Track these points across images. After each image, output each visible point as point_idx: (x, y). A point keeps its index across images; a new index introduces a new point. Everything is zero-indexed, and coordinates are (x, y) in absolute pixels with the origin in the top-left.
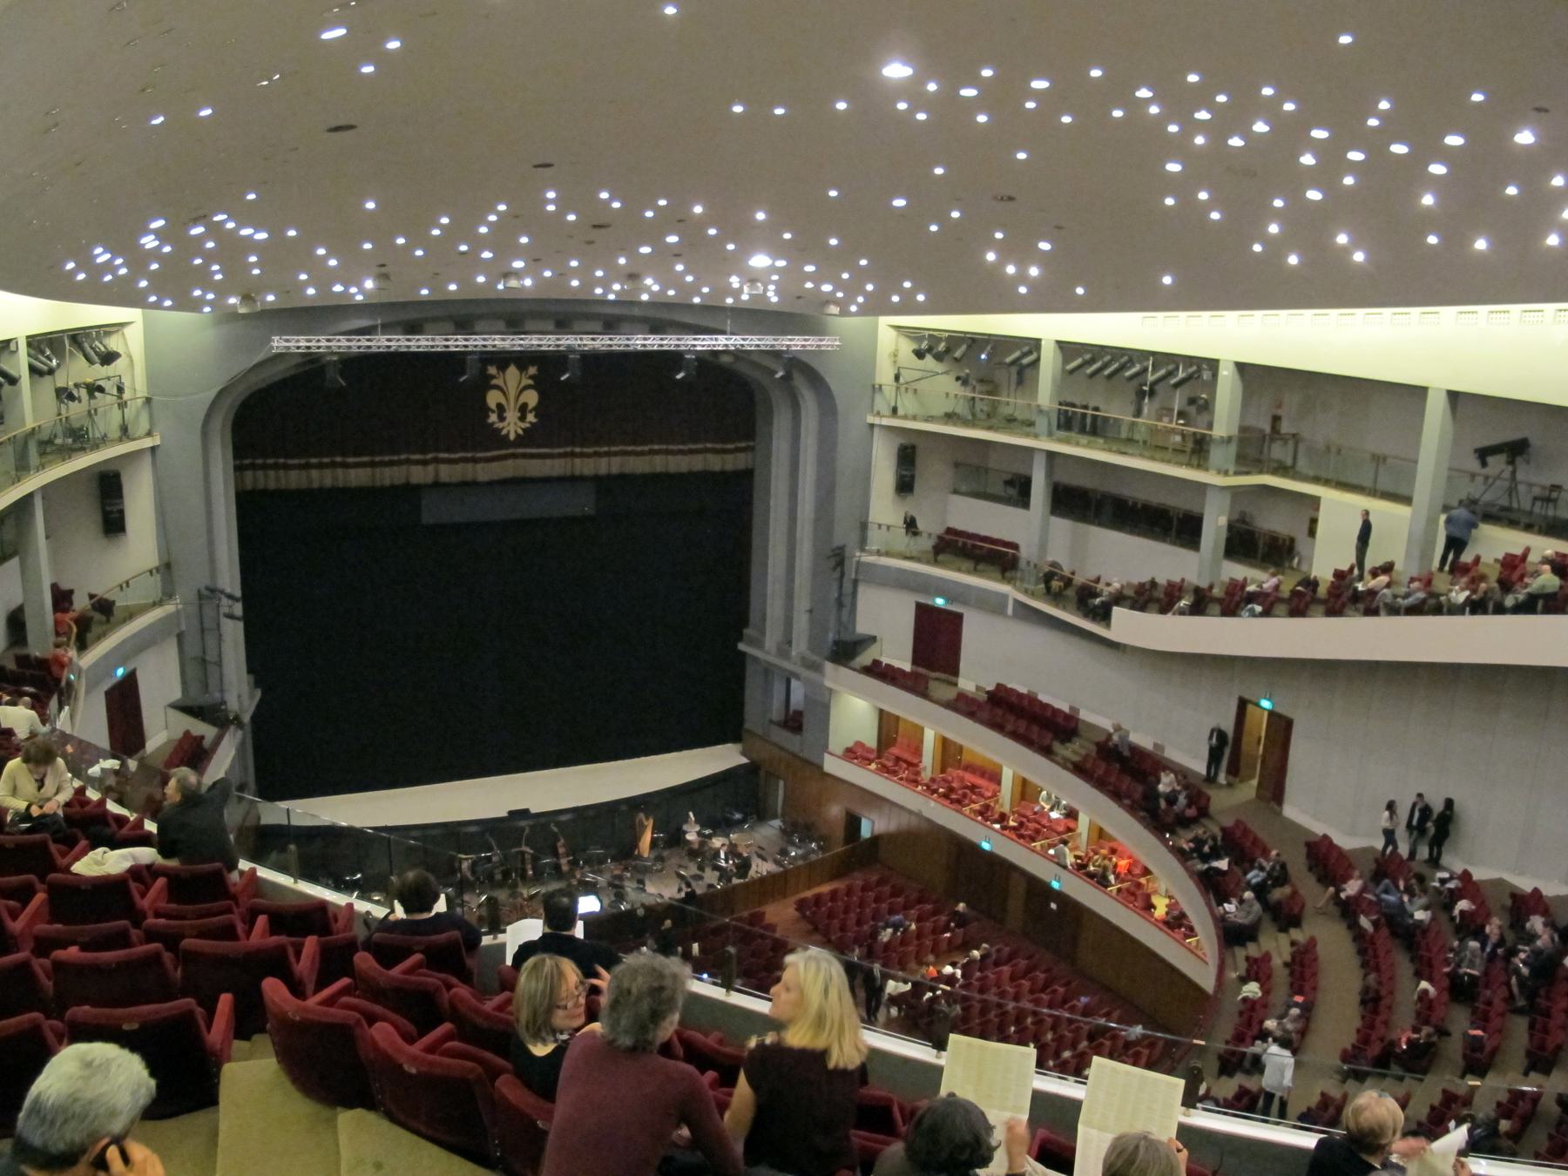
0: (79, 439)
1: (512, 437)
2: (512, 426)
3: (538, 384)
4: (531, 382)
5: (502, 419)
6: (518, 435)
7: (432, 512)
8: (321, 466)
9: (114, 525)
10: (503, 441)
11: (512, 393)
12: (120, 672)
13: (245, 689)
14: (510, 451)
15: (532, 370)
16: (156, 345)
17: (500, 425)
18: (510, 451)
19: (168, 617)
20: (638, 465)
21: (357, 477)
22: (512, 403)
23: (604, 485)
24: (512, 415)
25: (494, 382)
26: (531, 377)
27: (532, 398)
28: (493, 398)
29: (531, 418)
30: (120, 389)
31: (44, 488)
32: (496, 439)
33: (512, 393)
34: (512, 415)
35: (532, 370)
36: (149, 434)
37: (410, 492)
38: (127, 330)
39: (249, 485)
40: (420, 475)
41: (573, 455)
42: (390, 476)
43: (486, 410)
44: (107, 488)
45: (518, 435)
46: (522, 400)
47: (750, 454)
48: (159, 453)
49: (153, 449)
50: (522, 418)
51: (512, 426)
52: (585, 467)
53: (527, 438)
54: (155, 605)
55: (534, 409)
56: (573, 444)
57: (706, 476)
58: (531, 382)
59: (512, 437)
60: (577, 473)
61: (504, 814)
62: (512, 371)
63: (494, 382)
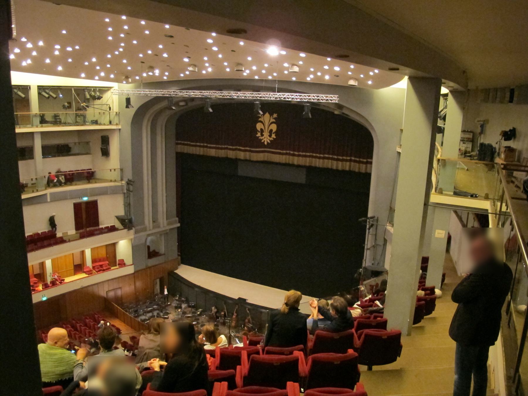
0: (96, 122)
1: (266, 143)
2: (266, 139)
3: (277, 122)
4: (274, 120)
5: (262, 135)
6: (268, 143)
7: (242, 171)
8: (200, 146)
9: (106, 153)
10: (262, 145)
11: (267, 124)
12: (85, 199)
13: (162, 220)
14: (266, 149)
15: (275, 115)
16: (116, 95)
17: (262, 138)
18: (266, 149)
19: (116, 187)
20: (318, 163)
21: (213, 152)
22: (267, 127)
23: (310, 169)
24: (266, 134)
25: (260, 119)
26: (274, 118)
27: (274, 127)
28: (259, 126)
29: (274, 136)
30: (110, 108)
31: (42, 133)
32: (260, 144)
33: (267, 124)
34: (266, 134)
35: (275, 115)
36: (117, 124)
37: (236, 161)
38: (112, 90)
39: (179, 150)
40: (231, 154)
41: (289, 154)
42: (222, 153)
43: (256, 131)
44: (105, 141)
45: (268, 143)
46: (270, 128)
47: (369, 165)
48: (121, 130)
49: (120, 129)
50: (270, 136)
51: (266, 139)
52: (296, 161)
53: (273, 144)
54: (111, 181)
55: (276, 132)
56: (290, 150)
57: (350, 173)
58: (274, 120)
59: (266, 143)
60: (291, 163)
61: (237, 298)
62: (267, 115)
63: (260, 119)
